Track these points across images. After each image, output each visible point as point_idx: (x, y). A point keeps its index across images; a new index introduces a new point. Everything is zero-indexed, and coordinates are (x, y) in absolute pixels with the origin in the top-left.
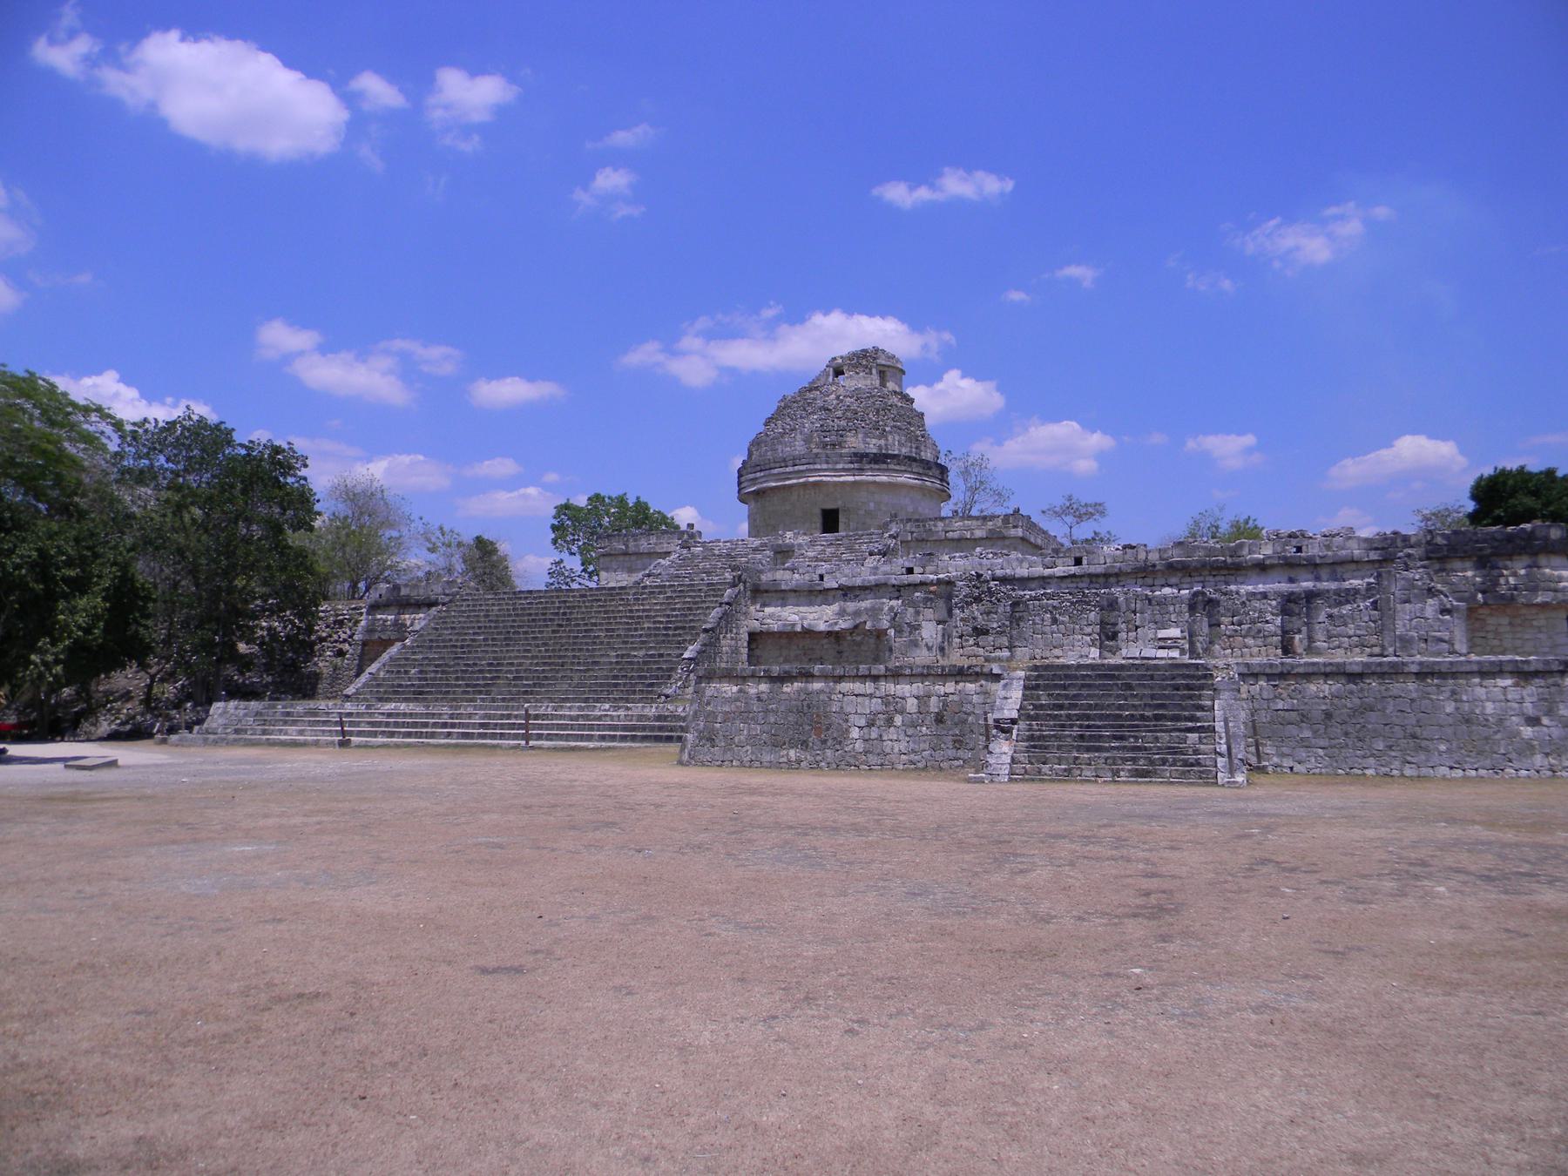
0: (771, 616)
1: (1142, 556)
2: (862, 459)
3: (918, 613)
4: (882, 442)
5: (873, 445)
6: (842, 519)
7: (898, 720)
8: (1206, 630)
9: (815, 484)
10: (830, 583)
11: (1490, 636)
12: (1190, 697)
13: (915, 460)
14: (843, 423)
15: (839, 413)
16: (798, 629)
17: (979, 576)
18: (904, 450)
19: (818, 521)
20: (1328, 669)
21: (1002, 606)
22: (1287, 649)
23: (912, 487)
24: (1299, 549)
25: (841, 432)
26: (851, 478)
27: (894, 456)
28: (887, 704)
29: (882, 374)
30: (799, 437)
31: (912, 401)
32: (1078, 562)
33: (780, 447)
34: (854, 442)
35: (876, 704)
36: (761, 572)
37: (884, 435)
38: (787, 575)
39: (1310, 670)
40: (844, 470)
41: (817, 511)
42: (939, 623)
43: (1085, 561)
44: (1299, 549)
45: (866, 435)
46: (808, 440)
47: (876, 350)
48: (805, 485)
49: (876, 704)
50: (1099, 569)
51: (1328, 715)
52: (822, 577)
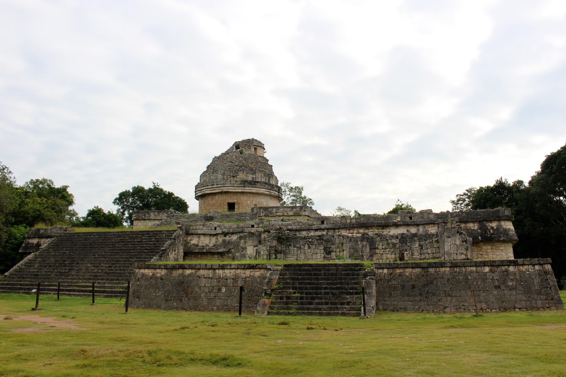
0: (194, 244)
1: (348, 221)
2: (244, 183)
3: (245, 242)
4: (254, 176)
6: (236, 206)
7: (224, 290)
8: (368, 250)
9: (226, 193)
10: (219, 231)
11: (484, 253)
12: (354, 279)
13: (267, 184)
14: (238, 168)
16: (205, 251)
17: (281, 228)
18: (263, 180)
19: (226, 207)
20: (414, 265)
21: (284, 240)
22: (402, 258)
23: (266, 195)
24: (411, 218)
25: (237, 172)
26: (240, 191)
27: (257, 182)
28: (219, 282)
29: (255, 149)
31: (268, 160)
32: (323, 222)
34: (242, 176)
35: (215, 283)
37: (254, 173)
39: (406, 266)
41: (226, 204)
42: (255, 246)
43: (325, 222)
44: (411, 218)
45: (247, 173)
46: (223, 175)
47: (253, 139)
48: (221, 193)
49: (215, 283)
50: (330, 226)
51: (413, 287)
52: (215, 229)
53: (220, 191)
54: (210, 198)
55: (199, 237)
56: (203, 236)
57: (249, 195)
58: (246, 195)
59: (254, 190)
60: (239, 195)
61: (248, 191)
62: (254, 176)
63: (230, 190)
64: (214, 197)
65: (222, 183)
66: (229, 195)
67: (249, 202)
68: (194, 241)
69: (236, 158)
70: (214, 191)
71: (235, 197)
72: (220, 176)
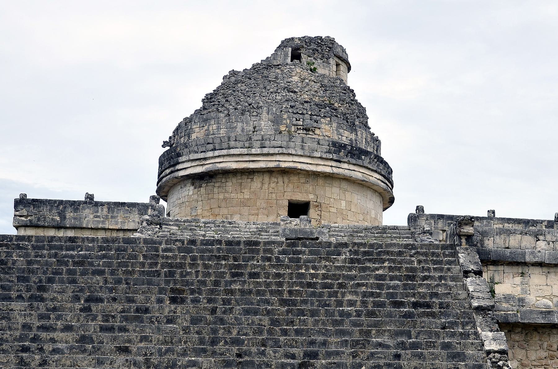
0: (508, 298)
4: (353, 136)
5: (346, 137)
6: (313, 213)
15: (306, 97)
19: (284, 213)
26: (328, 170)
29: (338, 65)
30: (264, 115)
33: (240, 125)
36: (484, 234)
38: (527, 242)
40: (321, 158)
45: (339, 127)
46: (276, 121)
48: (270, 171)
53: (272, 165)
54: (231, 184)
55: (523, 274)
56: (537, 270)
57: (344, 185)
58: (336, 183)
59: (358, 173)
60: (321, 181)
61: (347, 173)
62: (353, 136)
63: (299, 166)
64: (246, 181)
65: (279, 143)
66: (294, 179)
67: (343, 203)
68: (508, 285)
69: (302, 80)
70: (252, 166)
71: (309, 187)
72: (265, 124)
